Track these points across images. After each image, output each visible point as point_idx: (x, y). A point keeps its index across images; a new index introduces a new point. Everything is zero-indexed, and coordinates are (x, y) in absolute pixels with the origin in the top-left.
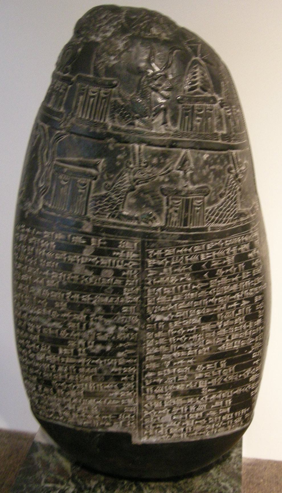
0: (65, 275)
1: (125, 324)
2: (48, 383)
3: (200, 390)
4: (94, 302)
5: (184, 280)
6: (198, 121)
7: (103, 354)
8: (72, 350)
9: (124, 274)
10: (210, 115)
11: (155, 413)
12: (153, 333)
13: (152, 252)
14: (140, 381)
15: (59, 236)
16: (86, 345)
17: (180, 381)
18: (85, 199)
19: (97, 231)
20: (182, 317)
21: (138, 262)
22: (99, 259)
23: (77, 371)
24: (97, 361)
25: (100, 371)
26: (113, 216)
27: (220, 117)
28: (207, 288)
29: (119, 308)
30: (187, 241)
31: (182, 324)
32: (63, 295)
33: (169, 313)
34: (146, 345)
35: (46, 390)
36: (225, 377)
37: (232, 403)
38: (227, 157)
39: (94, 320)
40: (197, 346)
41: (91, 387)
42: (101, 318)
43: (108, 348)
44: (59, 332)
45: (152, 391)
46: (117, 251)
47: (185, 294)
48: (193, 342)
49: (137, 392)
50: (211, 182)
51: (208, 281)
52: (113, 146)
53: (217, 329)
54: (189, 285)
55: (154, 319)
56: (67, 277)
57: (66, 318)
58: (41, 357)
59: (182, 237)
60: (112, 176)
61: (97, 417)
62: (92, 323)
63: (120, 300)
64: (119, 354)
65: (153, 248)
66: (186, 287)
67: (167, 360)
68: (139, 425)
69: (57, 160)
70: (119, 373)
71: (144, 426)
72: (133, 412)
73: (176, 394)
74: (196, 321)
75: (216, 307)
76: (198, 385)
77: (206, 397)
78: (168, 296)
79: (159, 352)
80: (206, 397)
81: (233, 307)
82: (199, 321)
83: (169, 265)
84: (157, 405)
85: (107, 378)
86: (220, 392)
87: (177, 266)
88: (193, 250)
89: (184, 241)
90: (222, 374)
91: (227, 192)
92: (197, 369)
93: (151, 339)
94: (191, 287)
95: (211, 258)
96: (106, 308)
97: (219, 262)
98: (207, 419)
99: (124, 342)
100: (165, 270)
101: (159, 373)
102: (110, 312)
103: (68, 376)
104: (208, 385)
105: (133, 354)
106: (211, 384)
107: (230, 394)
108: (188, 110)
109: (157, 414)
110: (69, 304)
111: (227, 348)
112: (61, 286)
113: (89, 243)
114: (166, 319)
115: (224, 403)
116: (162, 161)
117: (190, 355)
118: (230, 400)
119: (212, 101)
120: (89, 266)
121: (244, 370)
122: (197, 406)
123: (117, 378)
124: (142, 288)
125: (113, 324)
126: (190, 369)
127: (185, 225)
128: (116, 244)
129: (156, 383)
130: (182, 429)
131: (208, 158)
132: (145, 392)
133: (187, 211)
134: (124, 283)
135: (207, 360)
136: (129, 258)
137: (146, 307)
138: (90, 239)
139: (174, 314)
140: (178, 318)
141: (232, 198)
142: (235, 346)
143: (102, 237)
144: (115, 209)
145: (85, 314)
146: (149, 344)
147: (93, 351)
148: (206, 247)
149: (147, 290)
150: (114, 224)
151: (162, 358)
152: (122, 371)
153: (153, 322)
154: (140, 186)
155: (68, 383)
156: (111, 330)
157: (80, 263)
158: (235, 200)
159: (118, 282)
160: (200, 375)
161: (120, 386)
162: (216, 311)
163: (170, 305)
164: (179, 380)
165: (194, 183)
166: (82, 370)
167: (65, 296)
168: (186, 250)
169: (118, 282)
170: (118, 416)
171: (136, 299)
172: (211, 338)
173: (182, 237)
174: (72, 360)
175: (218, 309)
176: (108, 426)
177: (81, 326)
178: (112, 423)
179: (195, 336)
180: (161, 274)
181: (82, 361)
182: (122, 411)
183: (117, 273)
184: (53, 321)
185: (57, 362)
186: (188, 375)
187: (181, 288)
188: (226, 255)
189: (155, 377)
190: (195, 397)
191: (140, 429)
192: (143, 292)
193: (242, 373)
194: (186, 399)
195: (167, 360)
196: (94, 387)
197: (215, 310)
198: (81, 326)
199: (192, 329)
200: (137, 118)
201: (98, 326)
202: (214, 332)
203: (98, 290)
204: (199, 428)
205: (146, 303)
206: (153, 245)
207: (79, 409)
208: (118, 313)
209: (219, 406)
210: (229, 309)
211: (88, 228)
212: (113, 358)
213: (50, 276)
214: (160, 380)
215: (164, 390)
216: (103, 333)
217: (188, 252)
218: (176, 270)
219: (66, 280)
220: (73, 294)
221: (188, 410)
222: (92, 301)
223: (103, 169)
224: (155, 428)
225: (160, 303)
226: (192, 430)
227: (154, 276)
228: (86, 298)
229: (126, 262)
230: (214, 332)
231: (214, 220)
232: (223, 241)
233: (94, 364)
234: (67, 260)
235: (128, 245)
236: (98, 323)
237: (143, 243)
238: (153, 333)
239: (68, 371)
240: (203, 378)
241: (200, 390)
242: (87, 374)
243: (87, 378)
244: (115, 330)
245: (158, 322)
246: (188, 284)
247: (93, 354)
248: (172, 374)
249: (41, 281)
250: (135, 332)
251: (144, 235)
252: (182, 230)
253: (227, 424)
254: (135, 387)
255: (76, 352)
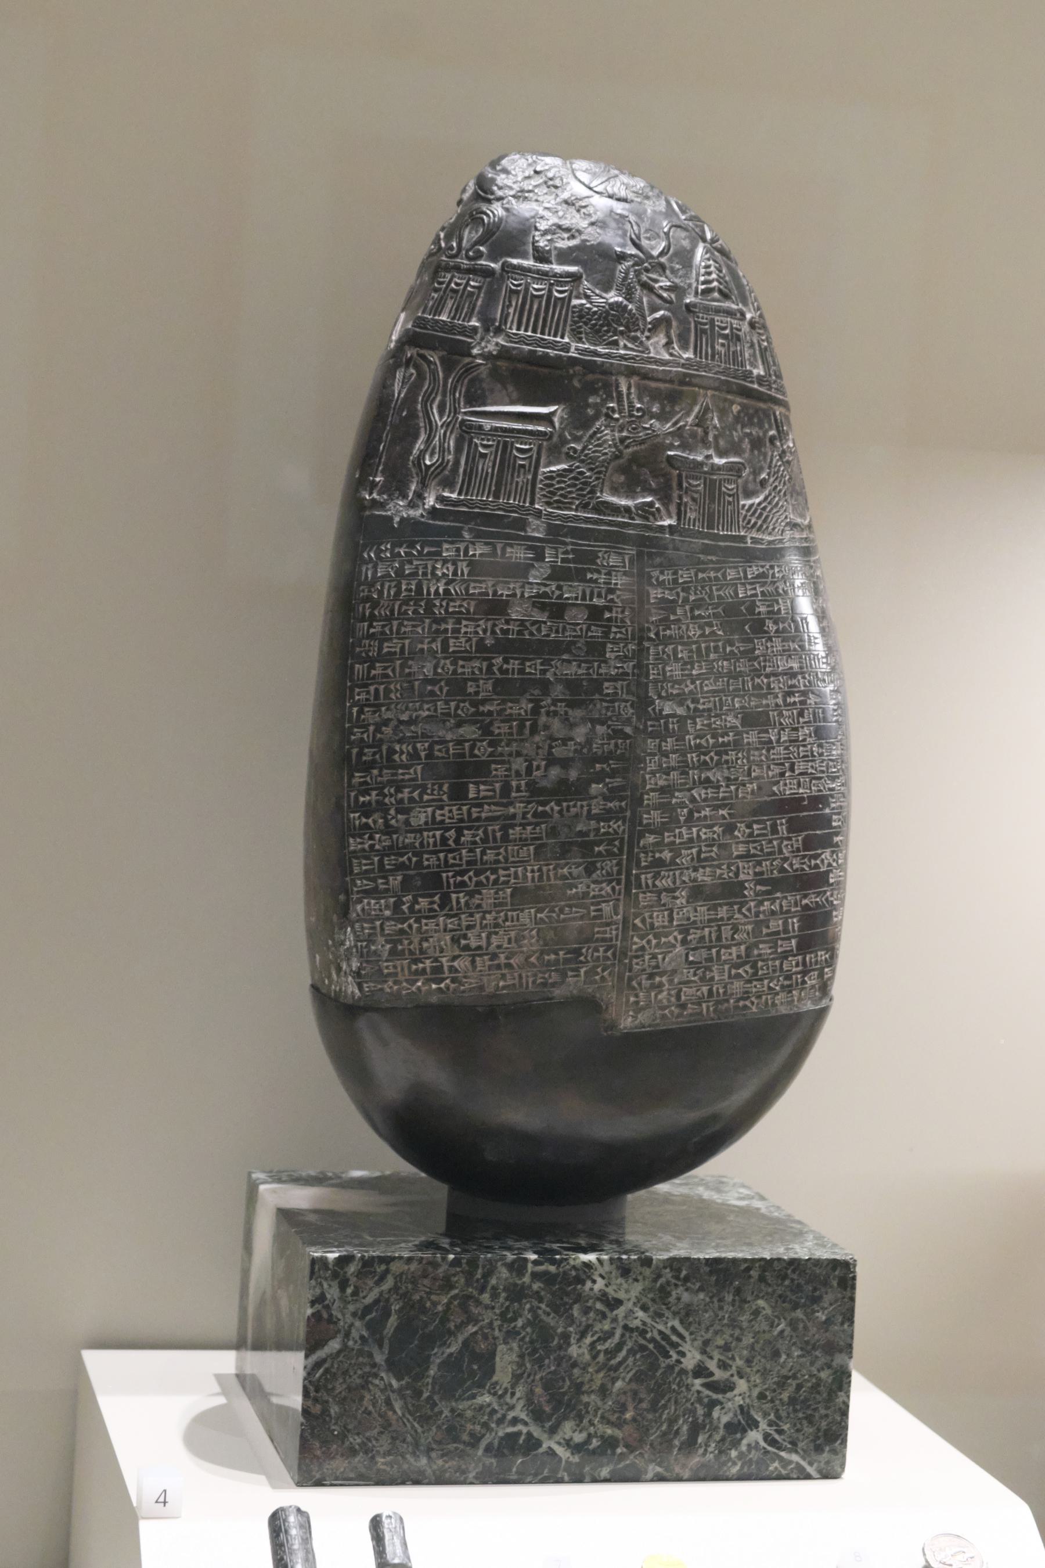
0: (490, 624)
1: (610, 718)
2: (432, 882)
3: (741, 885)
4: (549, 676)
5: (713, 633)
6: (723, 345)
7: (564, 791)
8: (497, 786)
9: (607, 615)
10: (738, 338)
11: (654, 942)
12: (657, 740)
13: (655, 573)
14: (630, 852)
15: (478, 550)
16: (529, 770)
17: (706, 859)
18: (530, 477)
19: (555, 533)
20: (709, 710)
21: (632, 591)
22: (559, 588)
23: (505, 838)
24: (547, 808)
25: (553, 832)
26: (585, 507)
27: (752, 346)
28: (749, 654)
29: (597, 685)
30: (714, 558)
31: (709, 725)
32: (485, 664)
33: (686, 699)
34: (645, 769)
35: (423, 903)
36: (785, 859)
37: (800, 929)
38: (766, 414)
39: (548, 713)
40: (736, 779)
41: (528, 874)
42: (561, 707)
43: (573, 774)
44: (472, 747)
45: (650, 882)
46: (592, 571)
47: (714, 660)
48: (728, 768)
49: (623, 886)
50: (747, 455)
51: (750, 641)
52: (580, 381)
53: (768, 745)
54: (720, 644)
55: (661, 711)
56: (495, 625)
57: (490, 713)
58: (419, 817)
59: (706, 550)
60: (580, 433)
61: (533, 959)
62: (543, 719)
63: (599, 667)
64: (595, 788)
65: (661, 565)
66: (716, 648)
67: (682, 805)
68: (621, 978)
69: (465, 413)
70: (592, 837)
71: (630, 979)
72: (611, 939)
73: (697, 893)
74: (732, 720)
75: (765, 696)
76: (737, 874)
77: (752, 904)
78: (686, 663)
79: (669, 786)
80: (752, 904)
81: (795, 703)
82: (737, 723)
83: (686, 600)
84: (659, 919)
85: (565, 850)
86: (778, 895)
87: (698, 604)
88: (724, 576)
89: (709, 558)
90: (781, 852)
91: (772, 480)
92: (736, 833)
93: (655, 755)
94: (724, 648)
95: (756, 595)
96: (572, 685)
97: (768, 606)
98: (754, 966)
99: (604, 759)
100: (679, 611)
101: (668, 838)
102: (580, 693)
103: (483, 853)
104: (756, 874)
105: (622, 788)
106: (762, 873)
107: (796, 905)
108: (706, 324)
109: (658, 945)
110: (497, 683)
111: (788, 792)
112: (481, 645)
113: (540, 557)
114: (680, 711)
115: (786, 923)
116: (668, 409)
117: (724, 798)
118: (795, 920)
119: (738, 315)
120: (540, 602)
121: (819, 851)
122: (735, 929)
123: (587, 848)
124: (640, 644)
125: (584, 720)
126: (724, 832)
127: (711, 526)
128: (589, 558)
129: (659, 863)
130: (705, 989)
131: (739, 412)
132: (639, 886)
133: (712, 500)
134: (606, 634)
135: (755, 812)
136: (616, 584)
137: (647, 685)
138: (544, 548)
139: (695, 701)
140: (704, 710)
141: (780, 491)
142: (801, 791)
143: (565, 544)
144: (589, 493)
145: (530, 701)
146: (652, 767)
147: (544, 783)
148: (745, 572)
149: (648, 648)
150: (587, 520)
151: (674, 801)
152: (598, 830)
153: (659, 716)
154: (630, 450)
155: (478, 873)
156: (580, 733)
157: (522, 595)
158: (785, 494)
159: (596, 632)
160: (742, 849)
161: (590, 870)
162: (768, 705)
163: (688, 682)
164: (703, 856)
165: (721, 454)
166: (515, 833)
167: (490, 666)
168: (712, 574)
169: (596, 632)
170: (577, 952)
171: (629, 666)
172: (760, 765)
173: (706, 550)
174: (498, 811)
175: (770, 701)
176: (553, 985)
177: (521, 727)
178: (564, 975)
179: (732, 755)
180: (672, 618)
181: (518, 808)
182: (588, 940)
183: (595, 614)
184: (459, 725)
185: (461, 820)
186: (720, 846)
187: (708, 648)
188: (779, 595)
189: (659, 845)
190: (731, 905)
191: (620, 992)
192: (642, 651)
193: (816, 857)
194: (714, 908)
195: (682, 805)
196: (537, 874)
197: (764, 702)
198: (521, 727)
199: (726, 739)
200: (622, 333)
201: (556, 724)
202: (764, 752)
203: (557, 648)
204: (737, 986)
205: (648, 675)
206: (658, 560)
207: (495, 941)
208: (597, 696)
209: (778, 933)
210: (790, 704)
211: (536, 530)
212: (581, 800)
213: (456, 631)
214: (667, 855)
215: (674, 883)
216: (565, 741)
217: (716, 578)
218: (697, 613)
219: (493, 632)
220: (506, 661)
221: (719, 938)
222: (544, 672)
223: (561, 423)
224: (653, 987)
225: (671, 676)
226: (725, 993)
227: (660, 620)
228: (533, 668)
229: (611, 591)
230: (764, 752)
231: (756, 523)
232: (772, 567)
233: (544, 814)
234: (495, 593)
235: (613, 560)
236: (556, 720)
237: (640, 554)
238: (657, 740)
239: (485, 840)
240: (746, 856)
241: (741, 885)
242: (523, 842)
243: (523, 853)
244: (588, 734)
245: (668, 716)
246: (719, 640)
247: (542, 791)
248: (691, 840)
249: (437, 646)
250: (627, 736)
251: (642, 542)
252: (707, 536)
253: (790, 986)
254: (619, 873)
255: (506, 789)
